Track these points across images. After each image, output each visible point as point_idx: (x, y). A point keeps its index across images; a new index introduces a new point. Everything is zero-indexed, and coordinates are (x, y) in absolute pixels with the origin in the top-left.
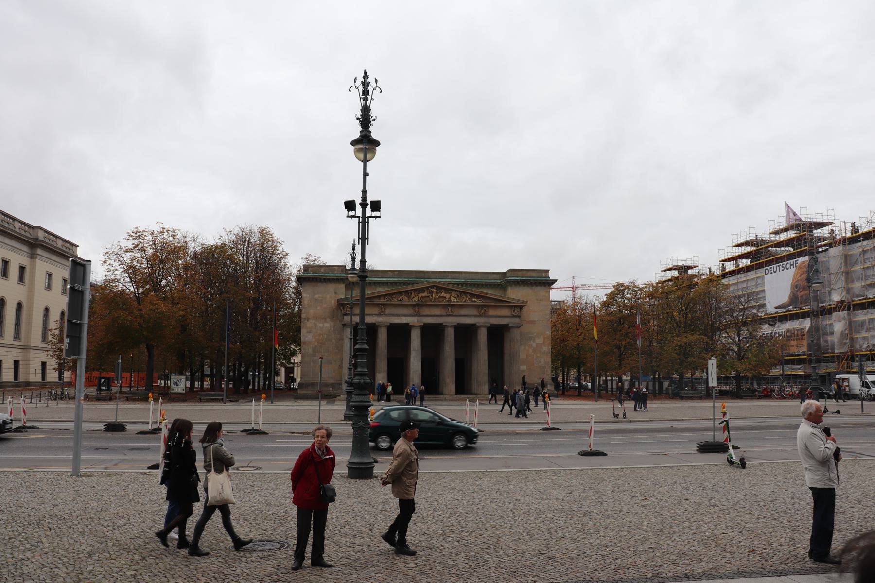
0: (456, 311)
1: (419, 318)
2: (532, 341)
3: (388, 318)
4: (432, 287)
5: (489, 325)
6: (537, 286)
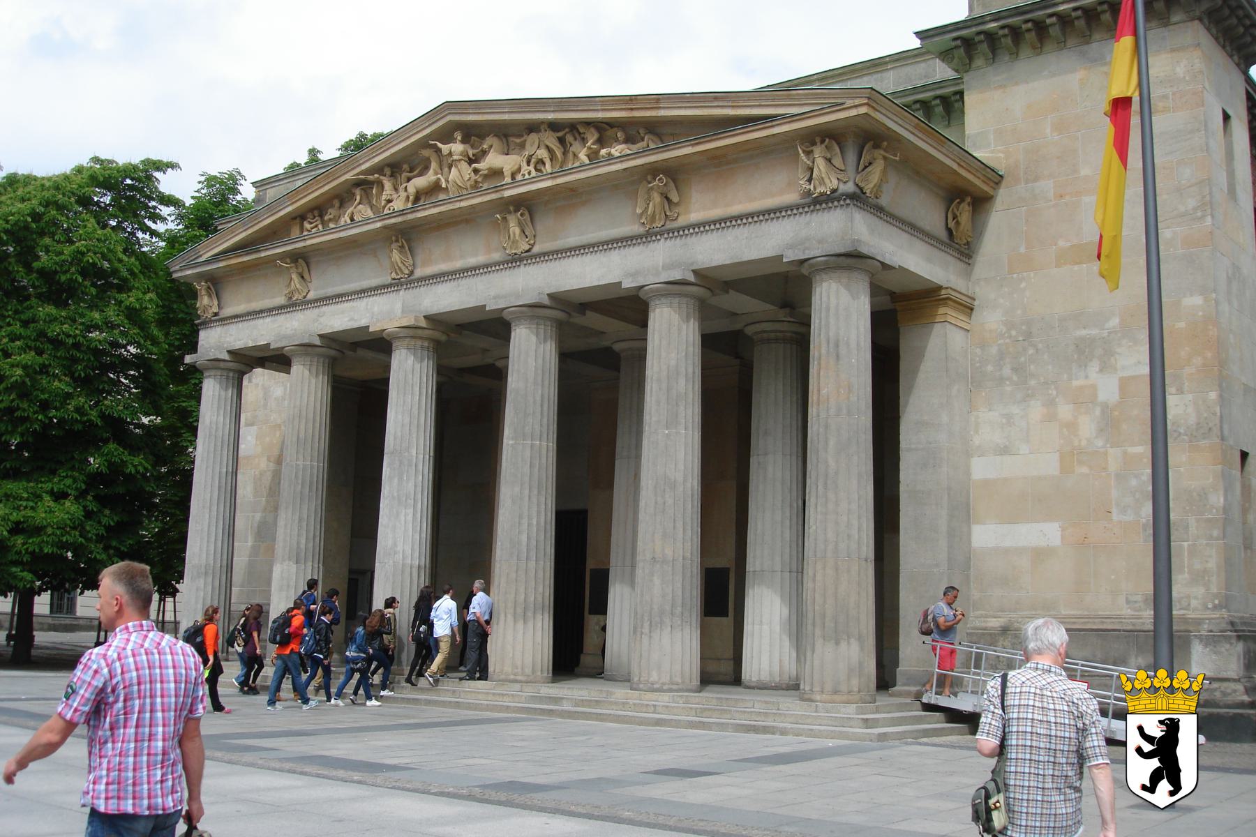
2: (1094, 367)
3: (316, 311)
4: (446, 135)
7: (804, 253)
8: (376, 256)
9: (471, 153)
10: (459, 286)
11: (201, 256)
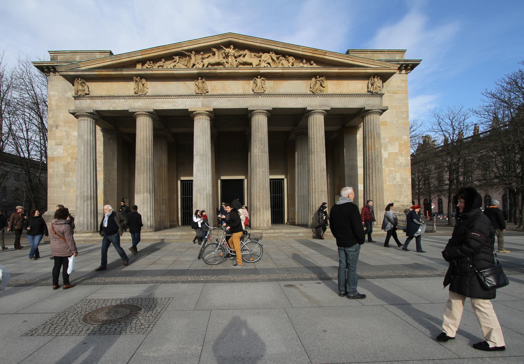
1: (206, 101)
5: (329, 109)
7: (372, 108)
8: (185, 84)
10: (230, 100)
11: (80, 67)
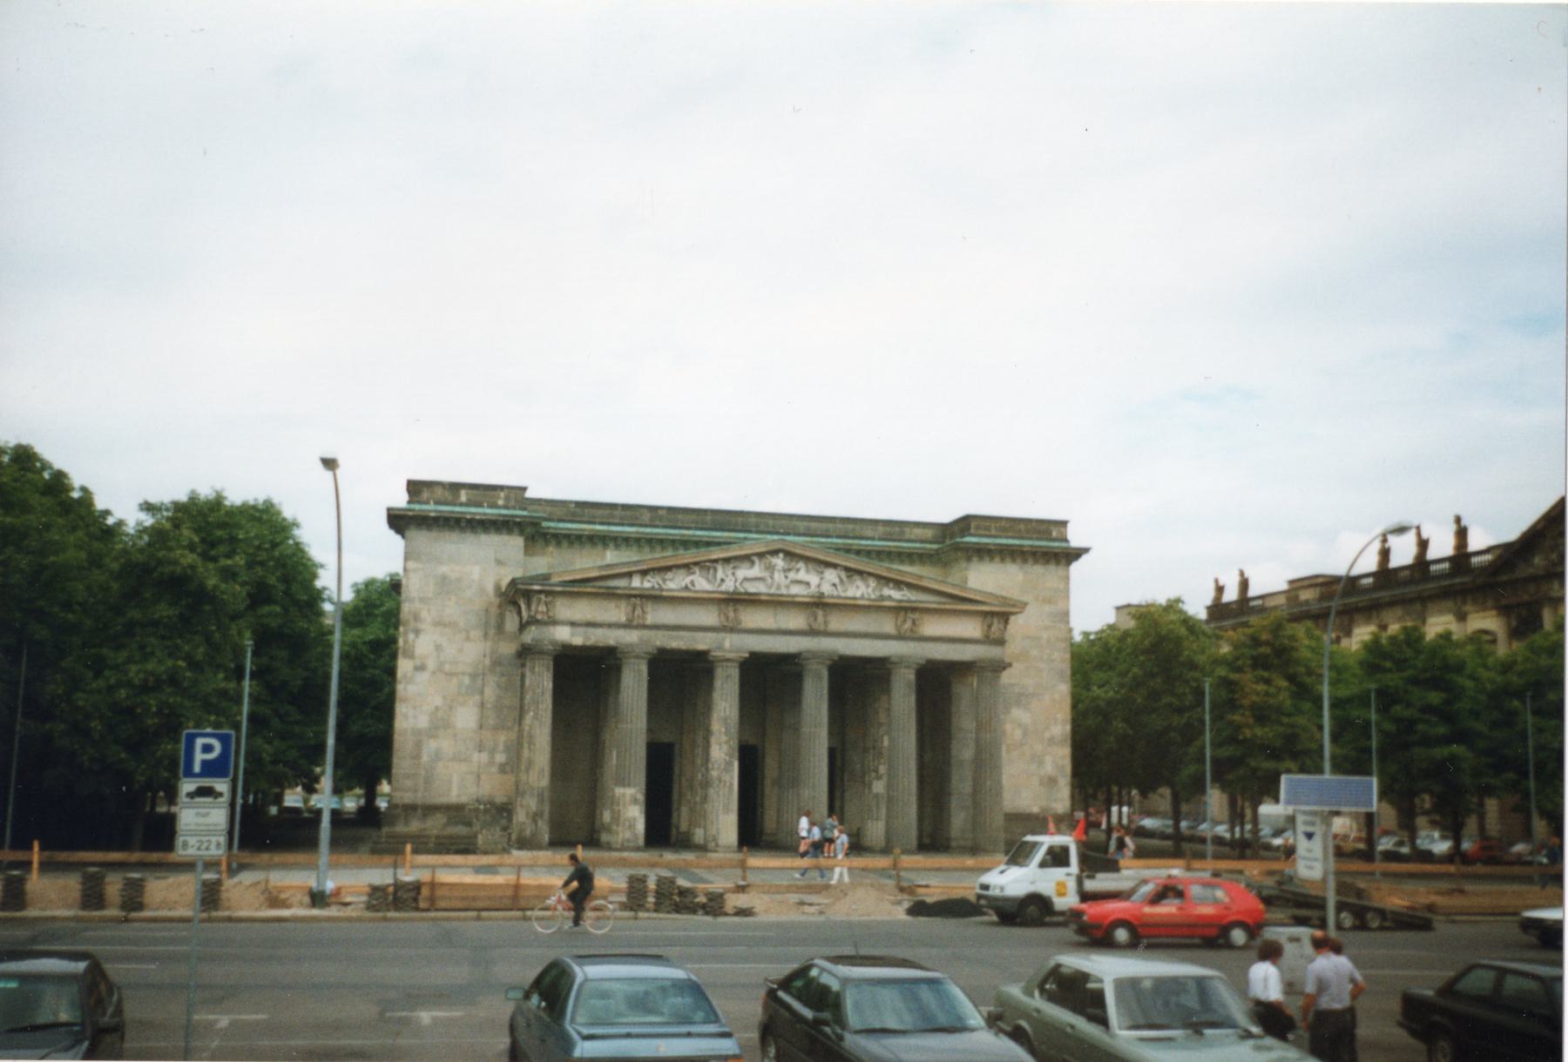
0: (837, 622)
4: (775, 553)
6: (1036, 562)
9: (786, 567)
